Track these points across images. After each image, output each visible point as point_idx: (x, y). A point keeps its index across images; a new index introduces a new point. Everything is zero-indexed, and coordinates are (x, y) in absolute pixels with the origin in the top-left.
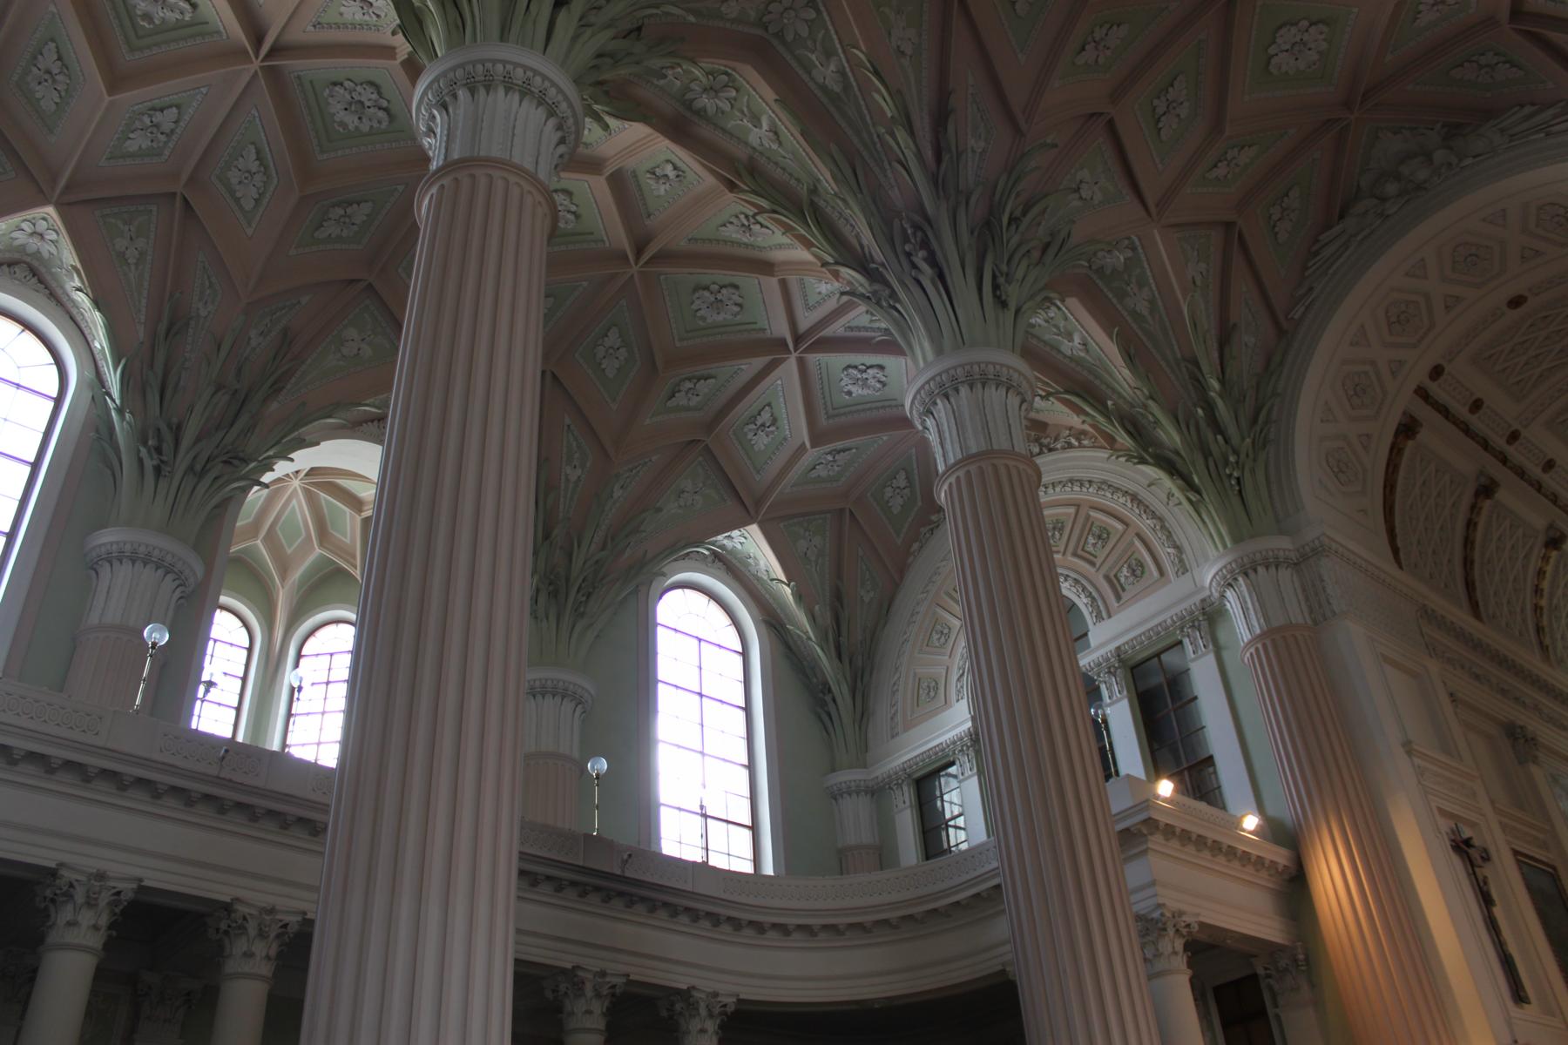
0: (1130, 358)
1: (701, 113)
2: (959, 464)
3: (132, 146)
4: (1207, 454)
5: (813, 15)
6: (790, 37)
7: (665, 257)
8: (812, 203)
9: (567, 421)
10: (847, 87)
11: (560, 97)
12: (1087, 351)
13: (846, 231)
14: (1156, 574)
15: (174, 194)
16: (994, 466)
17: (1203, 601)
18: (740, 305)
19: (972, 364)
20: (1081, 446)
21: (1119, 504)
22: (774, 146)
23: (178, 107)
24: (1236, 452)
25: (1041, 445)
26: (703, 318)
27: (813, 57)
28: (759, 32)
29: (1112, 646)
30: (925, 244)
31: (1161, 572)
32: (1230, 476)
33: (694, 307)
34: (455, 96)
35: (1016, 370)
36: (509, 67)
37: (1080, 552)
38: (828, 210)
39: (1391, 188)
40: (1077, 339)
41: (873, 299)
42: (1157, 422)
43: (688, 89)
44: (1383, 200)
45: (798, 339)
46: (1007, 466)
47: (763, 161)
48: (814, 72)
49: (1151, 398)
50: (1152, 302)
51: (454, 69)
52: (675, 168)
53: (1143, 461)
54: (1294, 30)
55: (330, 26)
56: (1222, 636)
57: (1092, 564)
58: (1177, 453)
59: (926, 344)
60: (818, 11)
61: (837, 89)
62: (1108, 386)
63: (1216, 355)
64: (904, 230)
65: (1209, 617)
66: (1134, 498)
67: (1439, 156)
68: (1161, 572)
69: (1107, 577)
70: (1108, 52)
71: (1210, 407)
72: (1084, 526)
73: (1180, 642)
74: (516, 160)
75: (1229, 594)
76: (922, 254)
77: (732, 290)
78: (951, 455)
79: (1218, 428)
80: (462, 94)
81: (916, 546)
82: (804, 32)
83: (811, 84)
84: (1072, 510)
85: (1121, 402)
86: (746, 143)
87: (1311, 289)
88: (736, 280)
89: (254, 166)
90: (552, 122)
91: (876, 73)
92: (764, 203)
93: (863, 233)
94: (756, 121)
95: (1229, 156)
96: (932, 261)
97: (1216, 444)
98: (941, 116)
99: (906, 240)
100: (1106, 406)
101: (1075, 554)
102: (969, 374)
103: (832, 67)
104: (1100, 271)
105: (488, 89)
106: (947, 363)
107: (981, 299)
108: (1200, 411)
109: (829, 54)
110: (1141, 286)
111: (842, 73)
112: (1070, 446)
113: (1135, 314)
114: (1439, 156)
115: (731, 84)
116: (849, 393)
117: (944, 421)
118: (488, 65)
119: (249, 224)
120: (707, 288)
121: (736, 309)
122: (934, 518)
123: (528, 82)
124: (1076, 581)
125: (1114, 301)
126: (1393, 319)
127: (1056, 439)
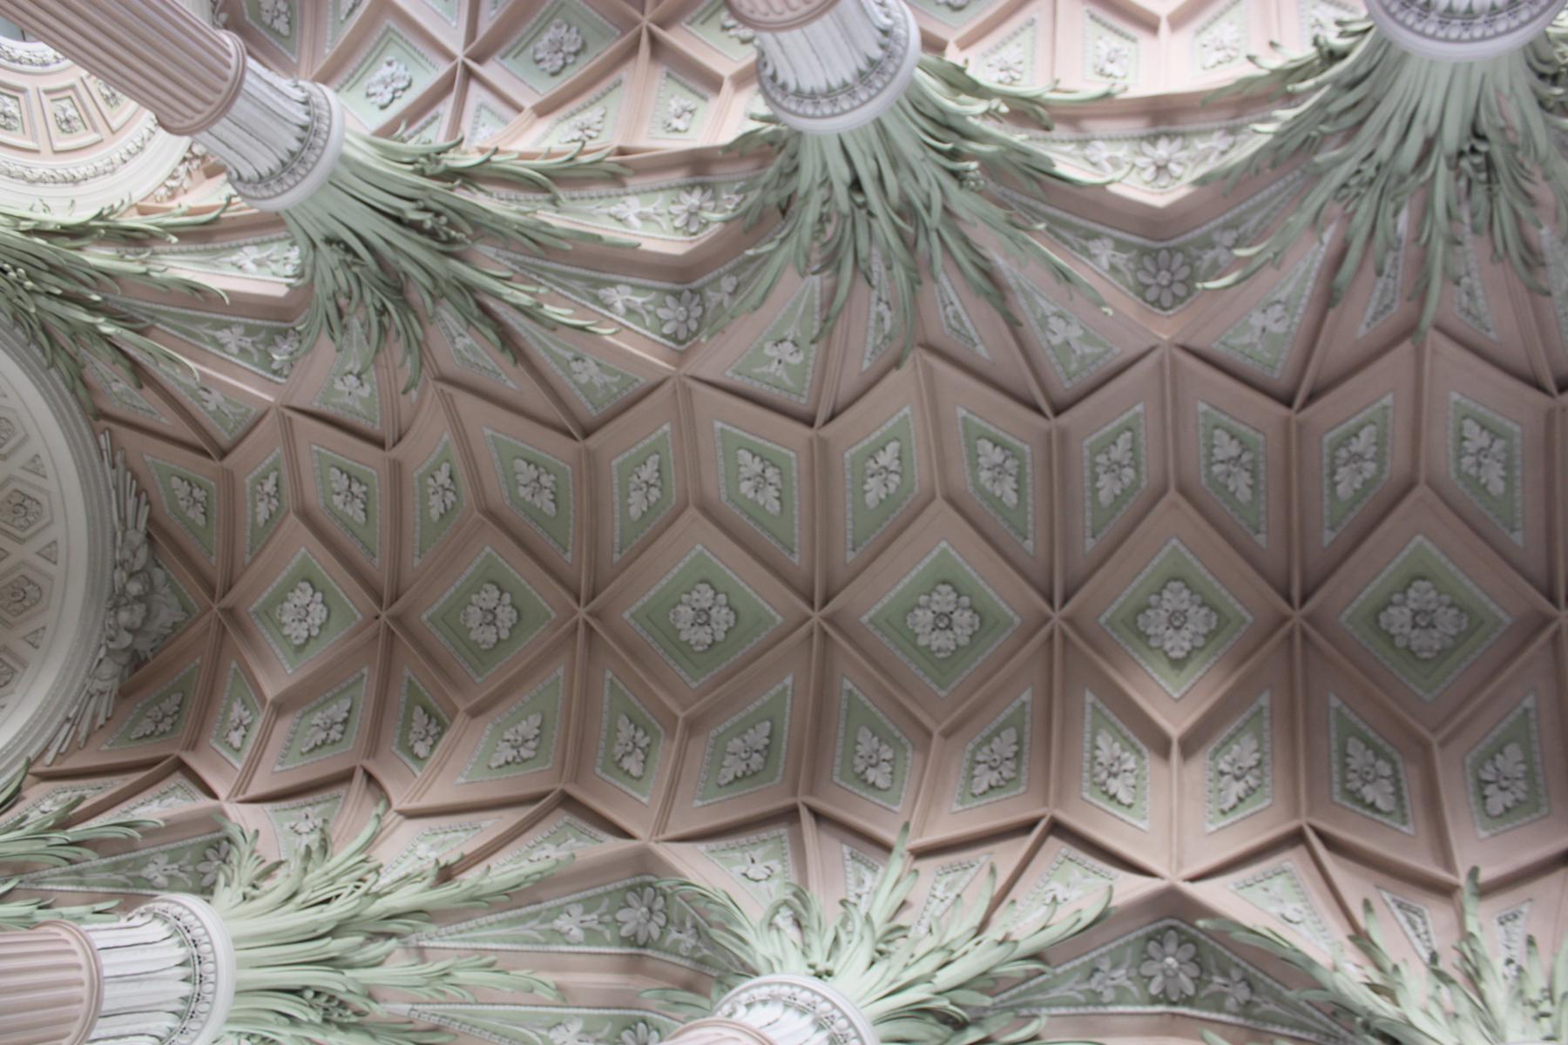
0: (195, 289)
1: (689, 188)
2: (239, 80)
4: (53, 269)
5: (666, 330)
6: (669, 299)
7: (631, 51)
8: (546, 190)
10: (596, 300)
11: (801, 110)
12: (233, 264)
13: (503, 191)
16: (209, 103)
18: (538, 62)
19: (309, 171)
20: (163, 184)
21: (79, 165)
22: (613, 210)
24: (31, 292)
25: (196, 157)
26: (558, 27)
27: (639, 300)
28: (695, 285)
30: (433, 234)
32: (15, 269)
33: (574, 30)
34: (882, 47)
35: (270, 198)
36: (856, 103)
37: (70, 93)
38: (530, 196)
39: (135, 588)
40: (250, 266)
41: (435, 155)
42: (122, 258)
43: (714, 198)
44: (131, 575)
45: (470, 74)
46: (199, 112)
48: (628, 289)
49: (146, 274)
50: (222, 346)
51: (898, 68)
52: (676, 130)
53: (99, 217)
54: (318, 622)
55: (1022, 29)
57: (48, 92)
58: (79, 249)
59: (360, 157)
60: (664, 336)
61: (602, 292)
62: (190, 252)
63: (132, 352)
64: (458, 230)
66: (75, 181)
67: (127, 639)
70: (431, 491)
71: (92, 308)
72: (90, 119)
74: (796, 33)
76: (428, 224)
77: (556, 68)
78: (254, 81)
79: (66, 298)
80: (877, 53)
82: (662, 313)
83: (624, 279)
84: (115, 124)
85: (167, 248)
86: (636, 194)
87: (114, 466)
88: (558, 80)
90: (792, 87)
91: (582, 329)
92: (585, 159)
93: (491, 202)
94: (644, 218)
95: (274, 501)
96: (416, 226)
97: (56, 285)
98: (507, 339)
99: (450, 224)
100: (176, 234)
101: (72, 87)
102: (303, 161)
103: (619, 305)
104: (284, 334)
105: (861, 74)
106: (328, 158)
107: (351, 229)
108: (96, 298)
109: (630, 312)
110: (242, 350)
111: (608, 307)
112: (172, 177)
113: (227, 326)
114: (127, 639)
115: (685, 229)
116: (390, 64)
117: (287, 105)
118: (873, 92)
120: (576, 54)
121: (539, 56)
122: (223, 17)
123: (834, 103)
124: (45, 64)
125: (250, 321)
126: (27, 503)
127: (189, 172)
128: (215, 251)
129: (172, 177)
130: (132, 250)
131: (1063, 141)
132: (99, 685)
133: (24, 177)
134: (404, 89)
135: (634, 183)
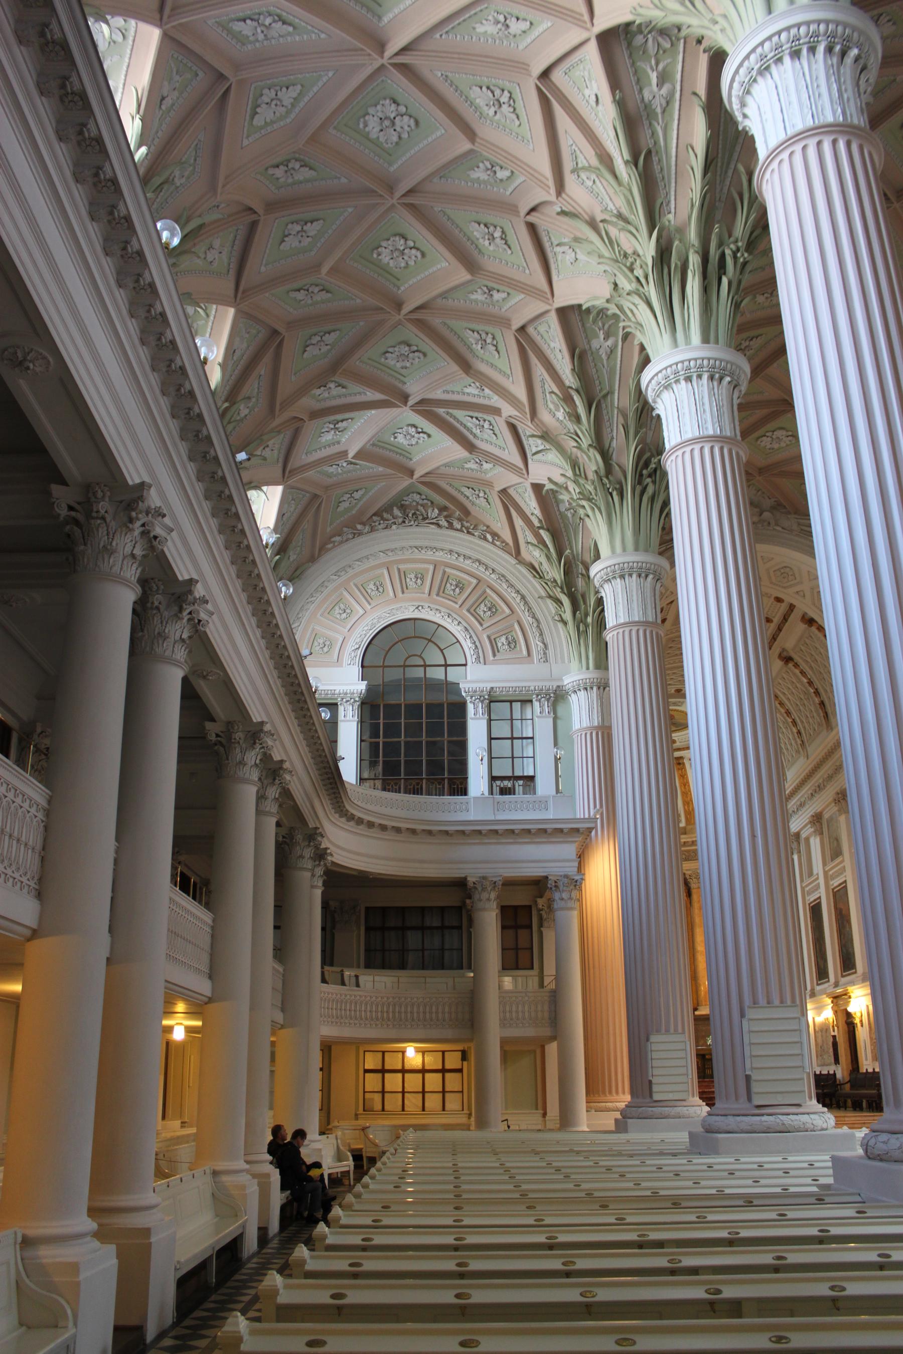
3: (238, 26)
8: (599, 402)
9: (262, 373)
13: (606, 431)
14: (525, 652)
15: (221, 77)
17: (558, 686)
20: (493, 543)
21: (510, 595)
22: (604, 357)
23: (295, 28)
25: (462, 526)
29: (489, 686)
31: (529, 654)
37: (472, 610)
47: (590, 358)
54: (784, 433)
56: (560, 710)
57: (481, 625)
59: (629, 533)
65: (557, 697)
66: (523, 598)
68: (529, 654)
69: (489, 637)
72: (480, 596)
73: (531, 701)
75: (582, 694)
81: (338, 539)
84: (475, 581)
86: (589, 342)
89: (287, 102)
94: (606, 338)
101: (468, 611)
112: (485, 539)
114: (766, 515)
119: (247, 137)
128: (566, 526)
129: (485, 539)
130: (575, 570)
131: (654, 134)
132: (795, 527)
133: (538, 626)
134: (416, 427)
135: (582, 344)
